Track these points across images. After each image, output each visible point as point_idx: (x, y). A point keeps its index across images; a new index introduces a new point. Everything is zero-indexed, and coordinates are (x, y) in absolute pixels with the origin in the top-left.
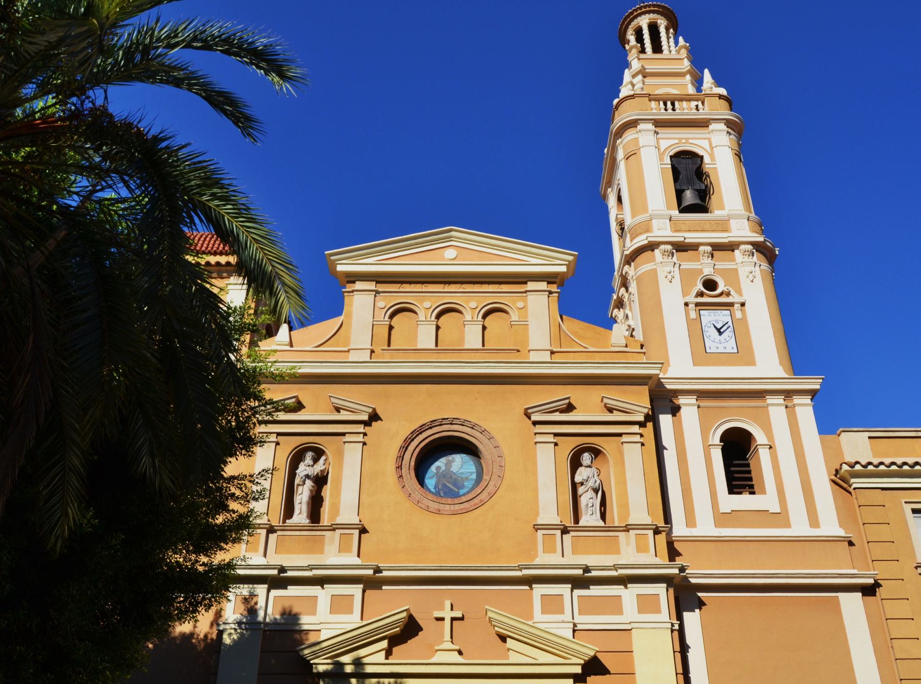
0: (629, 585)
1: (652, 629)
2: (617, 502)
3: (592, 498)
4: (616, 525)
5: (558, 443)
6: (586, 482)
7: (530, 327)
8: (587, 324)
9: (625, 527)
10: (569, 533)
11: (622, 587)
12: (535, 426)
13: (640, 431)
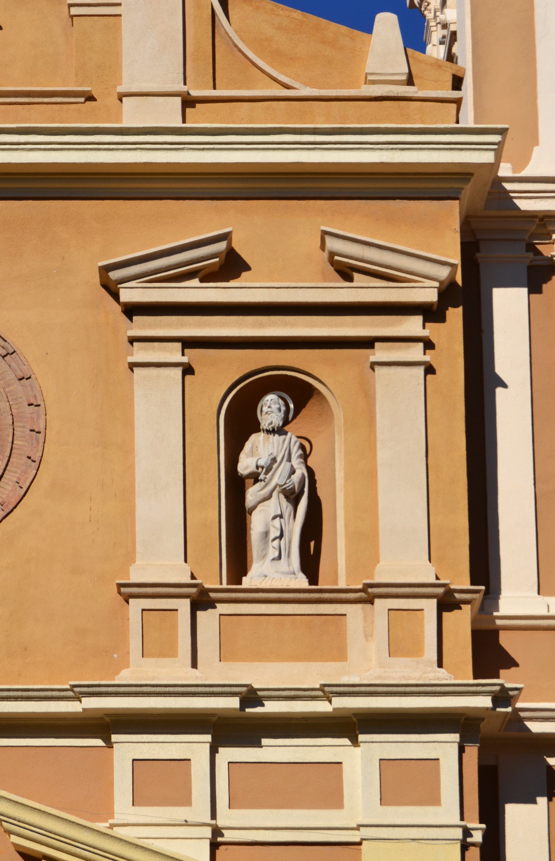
0: (362, 737)
1: (413, 843)
2: (346, 526)
3: (281, 516)
4: (342, 584)
5: (193, 365)
6: (266, 473)
7: (125, 21)
8: (297, 14)
9: (363, 590)
10: (215, 607)
11: (346, 741)
12: (131, 320)
13: (425, 333)
